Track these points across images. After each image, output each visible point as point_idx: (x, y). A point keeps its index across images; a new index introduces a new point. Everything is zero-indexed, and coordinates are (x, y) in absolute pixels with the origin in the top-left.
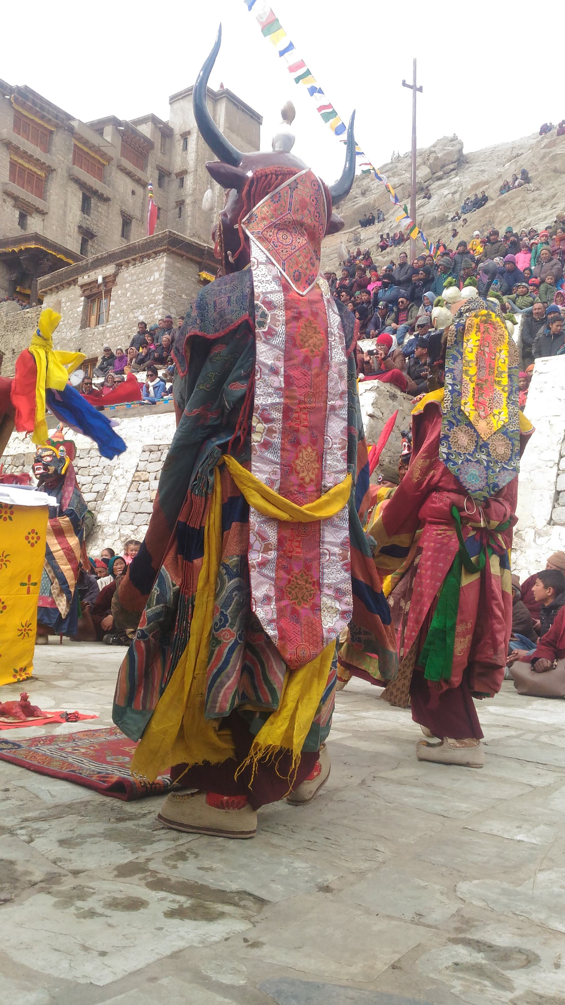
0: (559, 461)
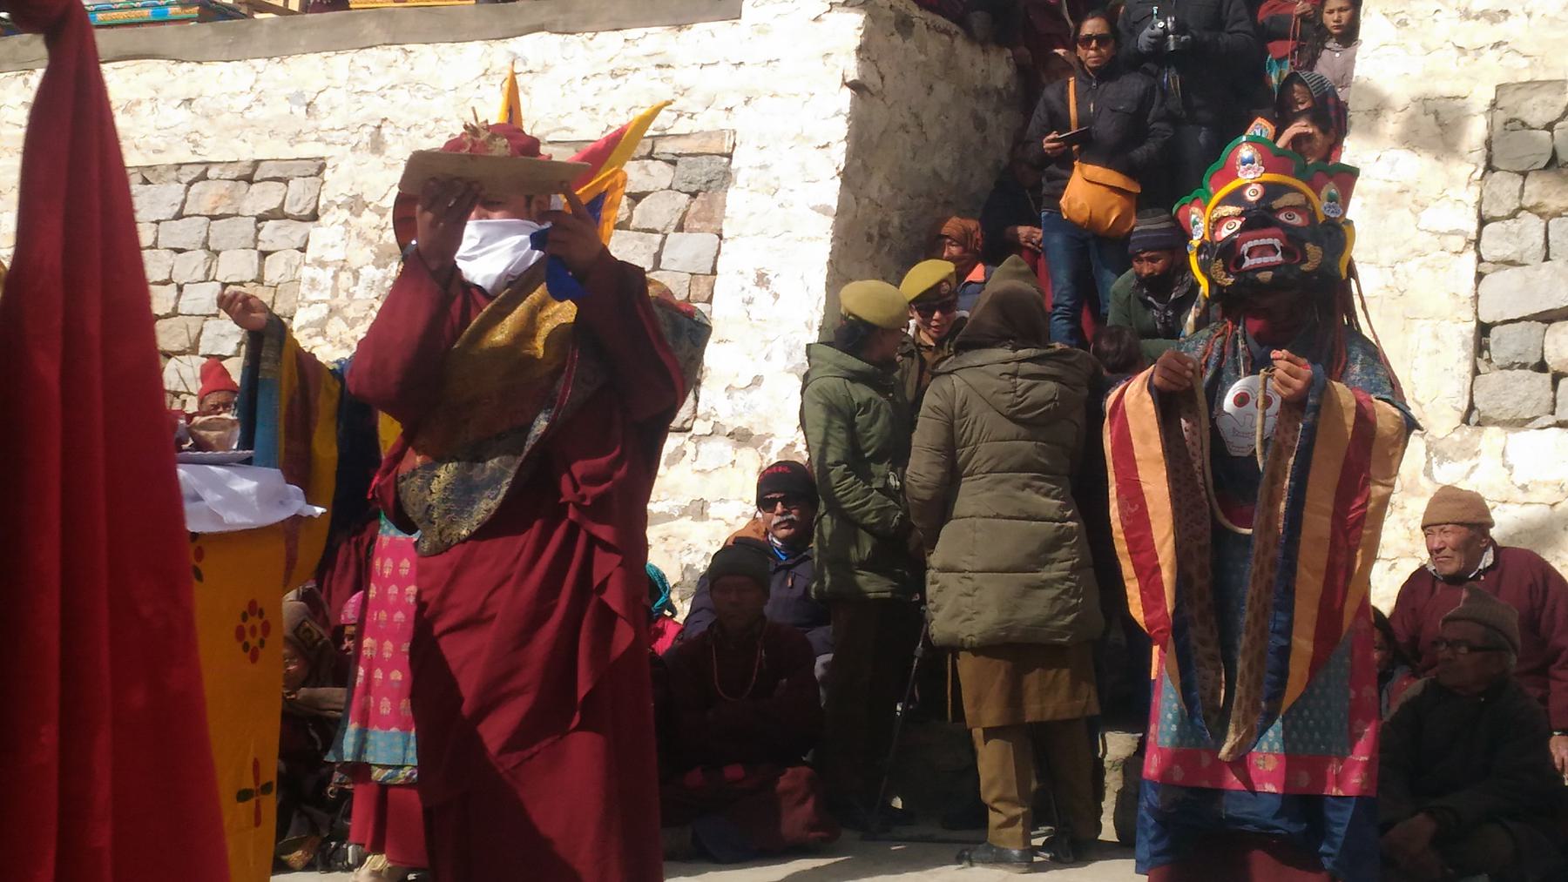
0: (1479, 233)
